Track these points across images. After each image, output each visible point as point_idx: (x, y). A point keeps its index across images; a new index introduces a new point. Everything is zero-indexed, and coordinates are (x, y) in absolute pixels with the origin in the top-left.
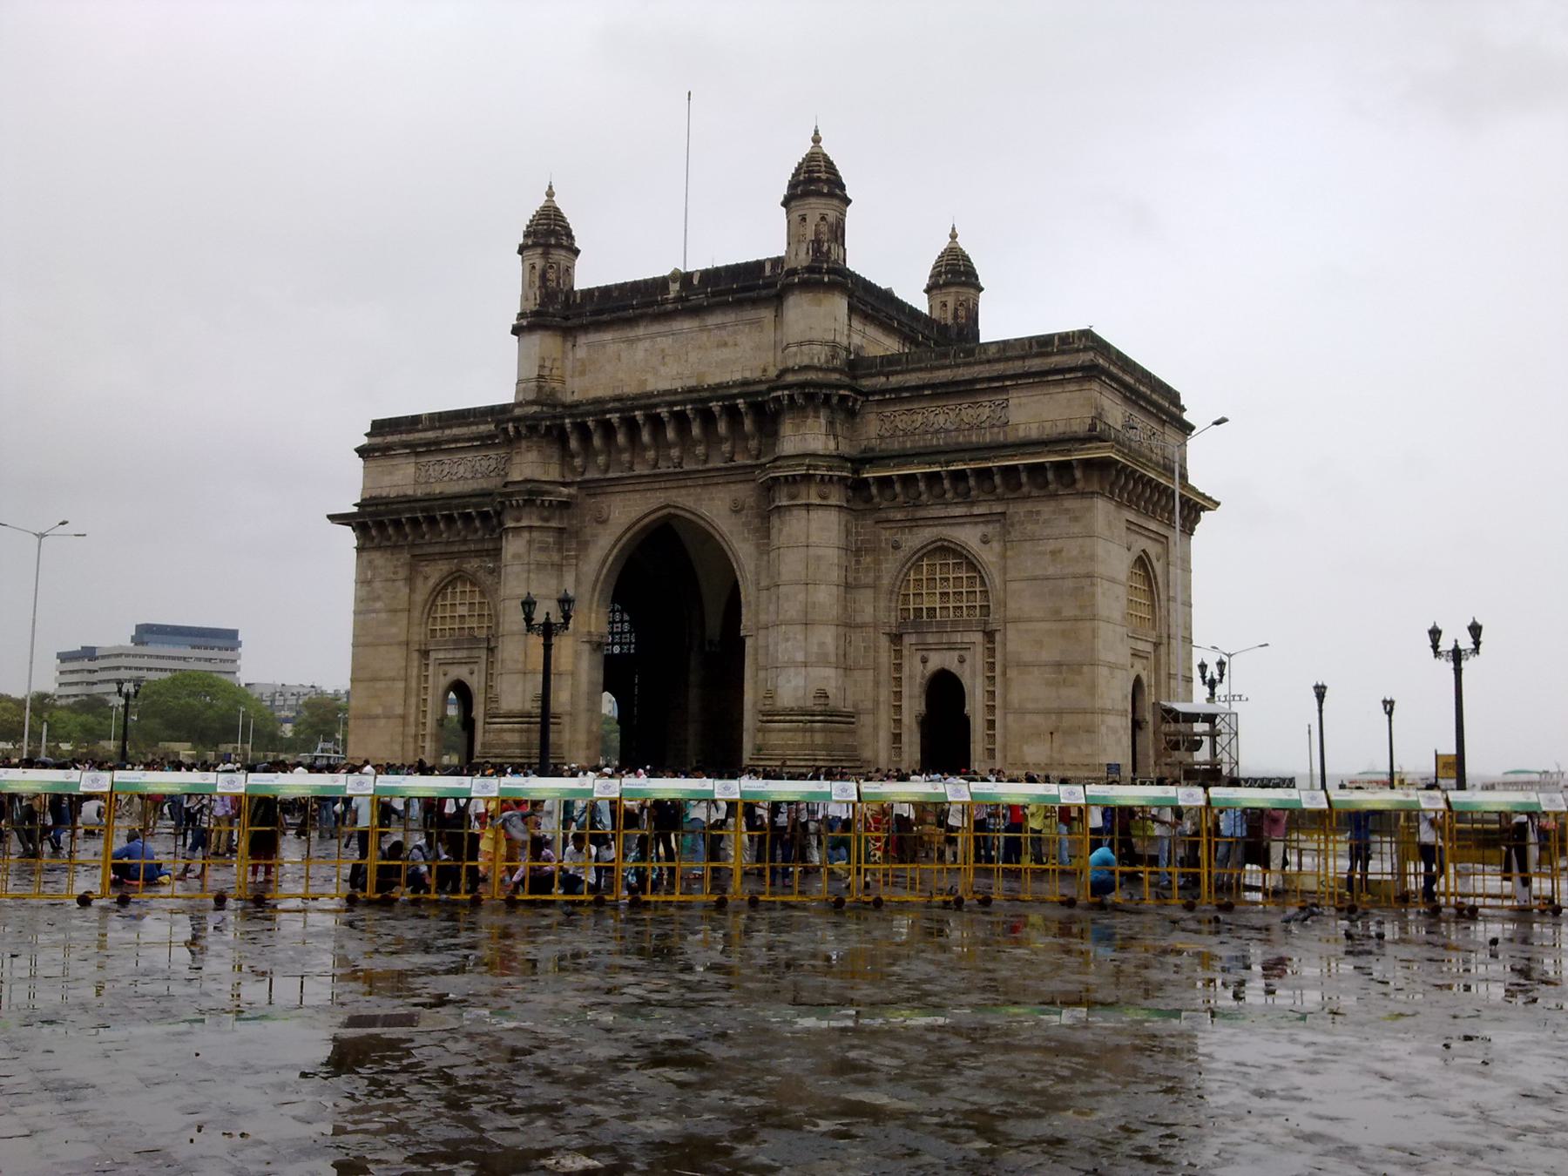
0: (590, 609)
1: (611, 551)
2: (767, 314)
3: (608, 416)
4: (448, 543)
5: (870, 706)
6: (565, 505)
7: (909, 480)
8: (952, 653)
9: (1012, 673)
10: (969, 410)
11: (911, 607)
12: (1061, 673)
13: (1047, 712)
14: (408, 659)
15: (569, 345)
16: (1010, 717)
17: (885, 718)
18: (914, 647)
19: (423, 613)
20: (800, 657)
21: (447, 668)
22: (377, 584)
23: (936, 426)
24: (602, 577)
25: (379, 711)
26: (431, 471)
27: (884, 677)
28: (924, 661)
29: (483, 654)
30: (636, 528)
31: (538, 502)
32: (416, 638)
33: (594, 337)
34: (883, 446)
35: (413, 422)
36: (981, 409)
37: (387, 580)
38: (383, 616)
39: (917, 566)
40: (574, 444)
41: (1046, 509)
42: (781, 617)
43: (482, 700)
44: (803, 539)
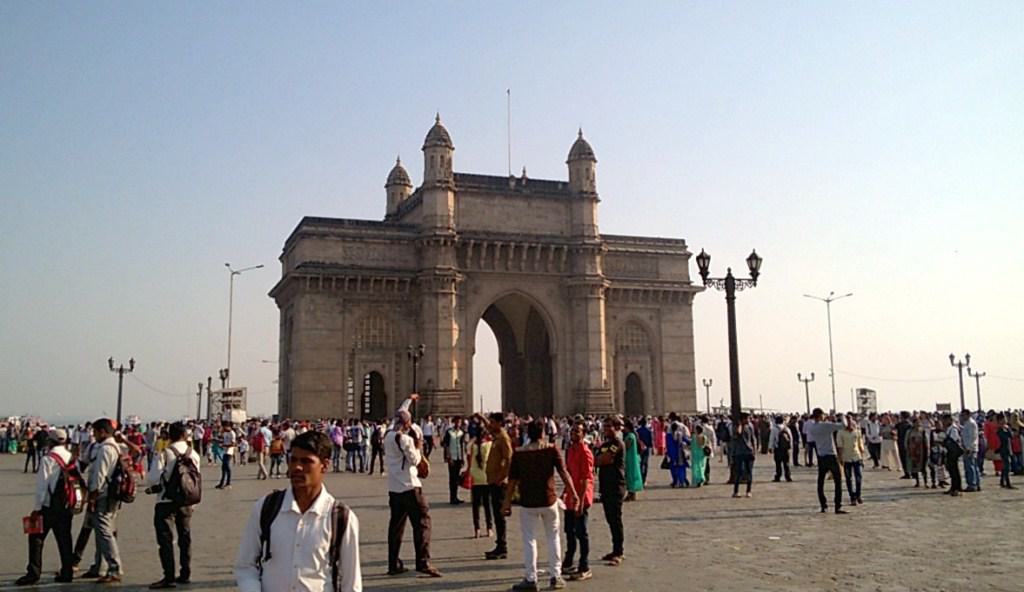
2: (562, 207)
3: (496, 243)
4: (370, 295)
9: (665, 374)
11: (619, 344)
13: (679, 390)
17: (612, 391)
22: (318, 314)
25: (324, 387)
28: (626, 367)
29: (393, 357)
33: (469, 199)
38: (324, 332)
40: (470, 253)
42: (591, 346)
43: (393, 381)
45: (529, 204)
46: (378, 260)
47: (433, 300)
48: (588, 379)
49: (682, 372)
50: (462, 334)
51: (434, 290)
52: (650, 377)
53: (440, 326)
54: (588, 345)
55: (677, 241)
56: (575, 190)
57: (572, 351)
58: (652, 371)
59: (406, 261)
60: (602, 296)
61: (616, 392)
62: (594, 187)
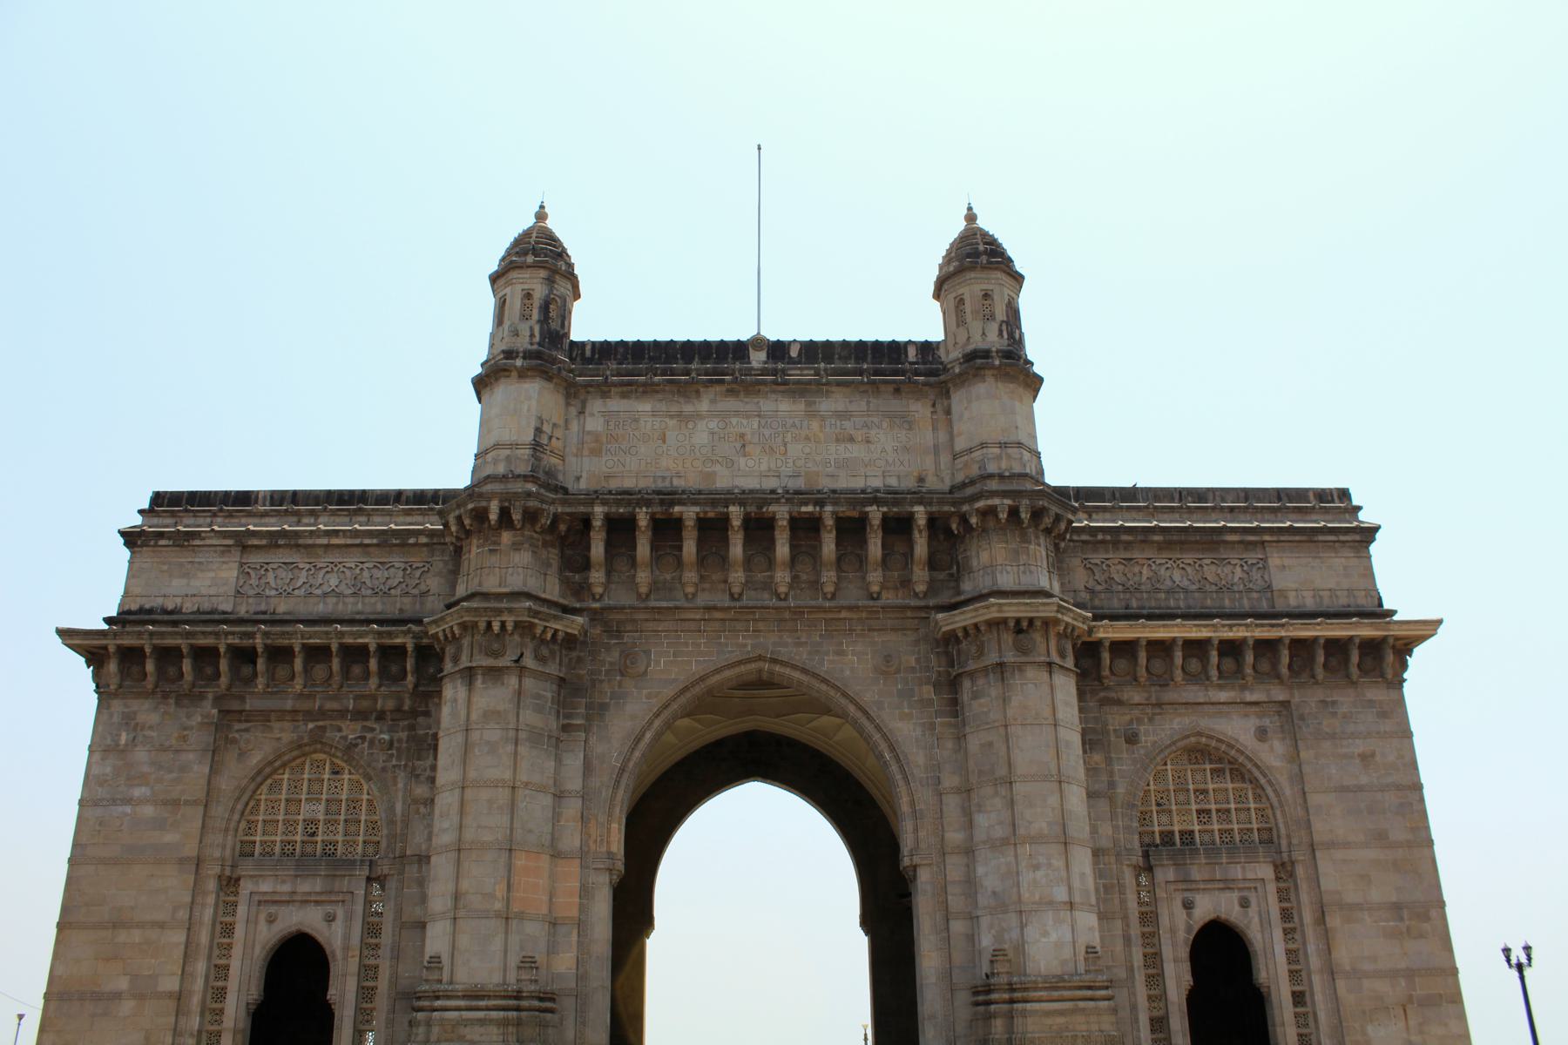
0: (610, 815)
1: (650, 723)
2: (920, 409)
5: (1122, 974)
6: (570, 641)
7: (1160, 648)
8: (1228, 894)
9: (1334, 921)
10: (1213, 568)
11: (1157, 829)
12: (1402, 919)
13: (1393, 974)
14: (197, 890)
15: (573, 411)
16: (1341, 984)
18: (1172, 887)
19: (233, 810)
20: (1061, 894)
21: (273, 909)
22: (141, 755)
23: (1168, 583)
24: (631, 764)
26: (271, 575)
27: (1135, 930)
28: (1188, 906)
30: (697, 690)
31: (538, 631)
32: (217, 854)
33: (616, 404)
34: (1097, 602)
35: (244, 499)
36: (1232, 567)
37: (163, 749)
38: (148, 811)
39: (1160, 776)
40: (598, 550)
41: (1345, 699)
42: (1021, 831)
44: (1047, 712)
45: (809, 404)
46: (339, 595)
47: (462, 693)
48: (1020, 948)
49: (1397, 908)
50: (572, 808)
51: (465, 662)
52: (1278, 934)
53: (472, 774)
54: (1014, 825)
55: (1322, 495)
56: (952, 356)
57: (969, 851)
58: (1286, 915)
59: (424, 594)
60: (1070, 662)
61: (1158, 997)
62: (1019, 342)
